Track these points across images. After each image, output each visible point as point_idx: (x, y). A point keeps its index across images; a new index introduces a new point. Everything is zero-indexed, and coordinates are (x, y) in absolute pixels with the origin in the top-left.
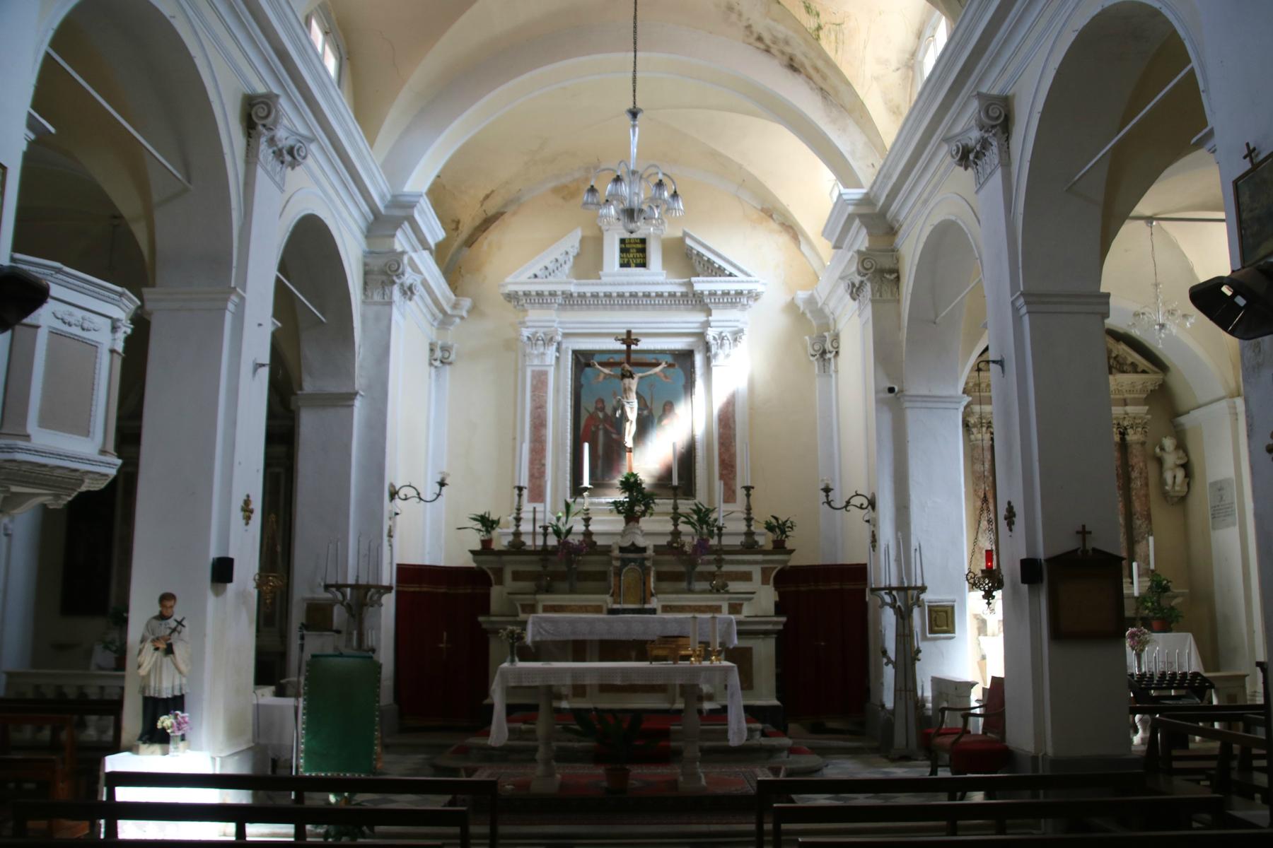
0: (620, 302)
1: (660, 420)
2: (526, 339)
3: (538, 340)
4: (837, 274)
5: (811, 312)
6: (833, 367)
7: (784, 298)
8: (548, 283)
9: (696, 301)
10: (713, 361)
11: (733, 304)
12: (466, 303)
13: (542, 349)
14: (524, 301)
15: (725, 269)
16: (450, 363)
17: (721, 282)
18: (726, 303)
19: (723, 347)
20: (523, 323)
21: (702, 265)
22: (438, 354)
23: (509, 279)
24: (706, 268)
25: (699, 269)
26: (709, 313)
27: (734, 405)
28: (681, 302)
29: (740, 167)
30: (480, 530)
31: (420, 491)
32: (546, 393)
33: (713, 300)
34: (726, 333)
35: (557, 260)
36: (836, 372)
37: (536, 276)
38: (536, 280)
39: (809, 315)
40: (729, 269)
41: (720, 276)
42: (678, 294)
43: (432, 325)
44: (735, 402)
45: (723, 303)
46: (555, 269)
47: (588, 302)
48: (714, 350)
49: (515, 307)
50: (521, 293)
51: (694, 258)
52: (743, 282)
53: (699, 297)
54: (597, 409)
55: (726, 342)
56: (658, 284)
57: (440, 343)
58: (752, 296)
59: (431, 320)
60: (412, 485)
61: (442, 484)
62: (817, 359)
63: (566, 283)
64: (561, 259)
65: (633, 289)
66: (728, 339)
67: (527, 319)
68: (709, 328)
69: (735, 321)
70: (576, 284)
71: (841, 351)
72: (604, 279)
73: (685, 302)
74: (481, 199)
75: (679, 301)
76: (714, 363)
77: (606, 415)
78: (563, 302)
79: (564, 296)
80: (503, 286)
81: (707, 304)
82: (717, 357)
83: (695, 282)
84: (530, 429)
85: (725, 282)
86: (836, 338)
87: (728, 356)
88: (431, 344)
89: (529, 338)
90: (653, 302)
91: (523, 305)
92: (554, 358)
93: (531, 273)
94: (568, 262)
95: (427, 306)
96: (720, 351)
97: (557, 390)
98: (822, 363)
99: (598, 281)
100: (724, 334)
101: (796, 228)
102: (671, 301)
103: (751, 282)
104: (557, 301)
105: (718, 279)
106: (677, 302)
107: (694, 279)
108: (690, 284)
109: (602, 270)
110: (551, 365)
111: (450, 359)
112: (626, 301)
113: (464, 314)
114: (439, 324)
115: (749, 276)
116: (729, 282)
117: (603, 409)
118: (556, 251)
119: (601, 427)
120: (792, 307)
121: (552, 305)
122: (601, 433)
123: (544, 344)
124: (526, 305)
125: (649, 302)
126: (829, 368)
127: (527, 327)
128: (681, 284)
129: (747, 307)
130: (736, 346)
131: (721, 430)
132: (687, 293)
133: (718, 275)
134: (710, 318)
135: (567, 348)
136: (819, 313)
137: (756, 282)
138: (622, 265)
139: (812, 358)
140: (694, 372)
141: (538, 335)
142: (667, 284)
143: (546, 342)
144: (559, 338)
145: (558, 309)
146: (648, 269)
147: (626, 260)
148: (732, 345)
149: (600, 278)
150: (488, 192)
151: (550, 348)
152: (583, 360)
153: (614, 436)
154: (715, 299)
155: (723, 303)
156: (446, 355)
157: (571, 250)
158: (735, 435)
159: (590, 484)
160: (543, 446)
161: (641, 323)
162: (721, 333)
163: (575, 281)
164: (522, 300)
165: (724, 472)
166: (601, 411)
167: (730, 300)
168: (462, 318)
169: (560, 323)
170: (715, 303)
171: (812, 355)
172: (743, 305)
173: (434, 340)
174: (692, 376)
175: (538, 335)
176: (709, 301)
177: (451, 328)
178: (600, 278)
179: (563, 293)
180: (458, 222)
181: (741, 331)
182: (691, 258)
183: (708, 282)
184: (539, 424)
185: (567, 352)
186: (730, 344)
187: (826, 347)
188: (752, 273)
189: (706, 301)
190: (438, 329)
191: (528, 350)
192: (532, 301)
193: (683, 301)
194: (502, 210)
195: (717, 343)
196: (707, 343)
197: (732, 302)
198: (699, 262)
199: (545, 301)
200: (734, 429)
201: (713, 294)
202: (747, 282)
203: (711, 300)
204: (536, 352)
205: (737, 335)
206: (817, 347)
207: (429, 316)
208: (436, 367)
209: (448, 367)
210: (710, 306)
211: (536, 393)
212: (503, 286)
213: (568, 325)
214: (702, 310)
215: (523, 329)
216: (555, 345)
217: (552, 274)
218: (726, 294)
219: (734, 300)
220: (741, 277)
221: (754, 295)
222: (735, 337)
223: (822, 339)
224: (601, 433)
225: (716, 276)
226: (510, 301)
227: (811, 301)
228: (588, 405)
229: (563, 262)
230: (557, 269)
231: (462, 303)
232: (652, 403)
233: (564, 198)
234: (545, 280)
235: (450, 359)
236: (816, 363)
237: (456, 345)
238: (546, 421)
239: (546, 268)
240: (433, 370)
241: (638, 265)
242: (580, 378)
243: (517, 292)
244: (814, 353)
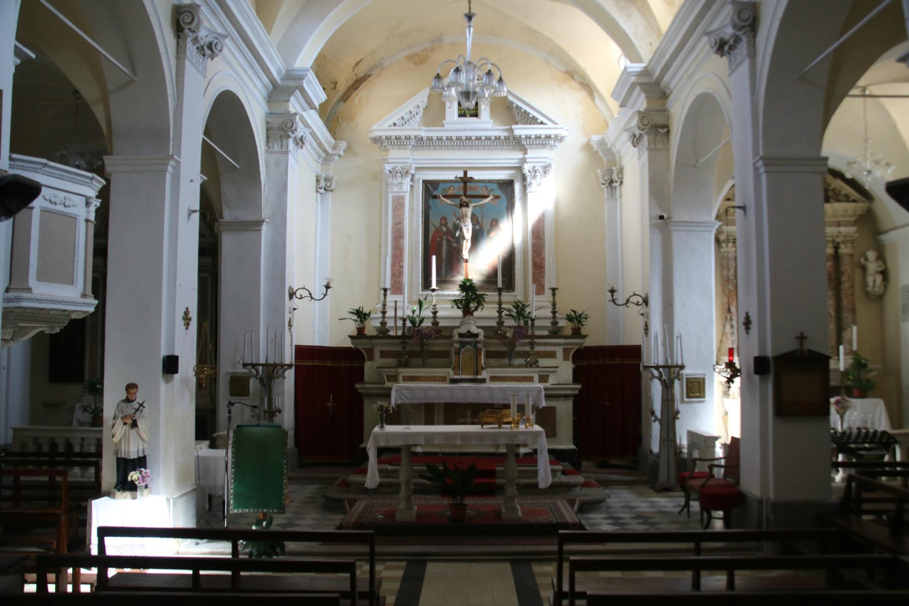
0: (458, 144)
1: (489, 232)
2: (388, 172)
3: (397, 173)
4: (622, 124)
5: (602, 151)
6: (618, 193)
7: (583, 140)
8: (404, 130)
9: (515, 143)
10: (528, 188)
11: (543, 145)
12: (343, 145)
13: (400, 180)
14: (386, 143)
15: (537, 119)
16: (331, 191)
17: (534, 128)
18: (538, 144)
19: (536, 178)
20: (385, 160)
21: (520, 116)
22: (323, 184)
23: (374, 127)
24: (523, 118)
25: (518, 118)
26: (525, 152)
27: (544, 222)
28: (504, 144)
29: (550, 39)
30: (356, 321)
31: (311, 292)
32: (404, 213)
33: (528, 143)
34: (539, 167)
35: (411, 112)
36: (621, 196)
37: (395, 124)
38: (395, 128)
39: (600, 154)
40: (541, 118)
41: (534, 124)
42: (502, 138)
43: (318, 162)
44: (544, 219)
45: (536, 144)
46: (410, 118)
47: (434, 144)
48: (529, 180)
49: (379, 148)
50: (384, 138)
51: (514, 109)
52: (551, 128)
53: (517, 140)
54: (441, 224)
55: (538, 174)
56: (487, 130)
57: (324, 175)
58: (558, 139)
59: (317, 159)
60: (305, 288)
61: (328, 287)
62: (606, 187)
63: (417, 130)
64: (414, 112)
65: (469, 134)
66: (539, 172)
67: (388, 157)
68: (525, 164)
69: (545, 158)
70: (425, 131)
71: (625, 182)
72: (446, 127)
73: (508, 144)
74: (353, 66)
75: (503, 143)
76: (529, 190)
77: (448, 229)
78: (416, 144)
79: (417, 139)
80: (370, 132)
81: (524, 146)
82: (531, 185)
83: (515, 129)
84: (392, 240)
85: (538, 128)
86: (621, 171)
87: (539, 184)
88: (317, 176)
89: (390, 171)
90: (483, 144)
91: (385, 146)
92: (409, 186)
93: (391, 122)
94: (419, 114)
95: (313, 148)
96: (533, 181)
97: (411, 210)
98: (610, 191)
99: (442, 128)
100: (536, 168)
101: (591, 87)
102: (497, 143)
103: (557, 128)
104: (411, 143)
105: (532, 126)
106: (501, 144)
107: (514, 127)
108: (511, 130)
109: (445, 119)
110: (407, 192)
111: (331, 188)
112: (463, 143)
113: (342, 153)
114: (322, 161)
115: (556, 124)
116: (541, 128)
117: (446, 225)
118: (410, 106)
119: (444, 238)
120: (588, 147)
121: (407, 146)
122: (444, 243)
123: (402, 176)
124: (388, 146)
125: (480, 144)
126: (615, 193)
127: (389, 163)
128: (504, 130)
129: (554, 147)
130: (546, 177)
131: (534, 241)
132: (509, 136)
133: (532, 123)
134: (526, 156)
135: (419, 178)
136: (609, 152)
137: (560, 128)
138: (460, 116)
139: (602, 186)
140: (514, 197)
141: (397, 169)
142: (493, 130)
143: (403, 175)
144: (413, 171)
145: (412, 149)
146: (480, 118)
147: (463, 111)
148: (542, 176)
149: (443, 126)
150: (358, 60)
151: (406, 179)
152: (430, 188)
153: (454, 245)
154: (530, 142)
155: (536, 144)
156: (329, 184)
157: (422, 104)
158: (544, 244)
159: (437, 286)
160: (401, 253)
161: (475, 159)
162: (534, 167)
163: (424, 128)
164: (385, 142)
165: (536, 272)
167: (541, 142)
168: (340, 156)
169: (414, 159)
170: (530, 144)
171: (603, 184)
172: (551, 146)
173: (320, 173)
174: (512, 201)
175: (397, 169)
176: (525, 143)
177: (332, 164)
178: (443, 126)
179: (416, 137)
180: (336, 83)
181: (550, 165)
182: (512, 110)
183: (524, 128)
184: (398, 236)
185: (419, 182)
186: (541, 175)
187: (613, 178)
188: (558, 122)
189: (523, 143)
190: (322, 164)
191: (390, 181)
192: (393, 143)
193: (506, 143)
194: (369, 73)
195: (531, 175)
196: (524, 175)
197: (542, 144)
198: (518, 113)
199: (402, 143)
200: (544, 240)
201: (528, 137)
202: (554, 128)
203: (527, 142)
204: (395, 182)
205: (546, 169)
206: (606, 178)
207: (315, 156)
208: (321, 194)
209: (330, 193)
210: (526, 146)
211: (396, 213)
212: (370, 132)
213: (419, 162)
214: (520, 150)
215: (386, 165)
216: (410, 176)
217: (407, 123)
218: (538, 137)
219: (544, 142)
220: (550, 125)
221: (559, 138)
222: (545, 170)
223: (610, 171)
224: (444, 243)
225: (530, 124)
226: (376, 143)
227: (602, 143)
228: (435, 221)
229: (415, 114)
230: (411, 118)
231: (340, 145)
232: (482, 220)
233: (415, 63)
234: (401, 127)
235: (331, 188)
236: (605, 190)
237: (336, 177)
238: (403, 234)
239: (403, 118)
240: (319, 195)
241: (472, 116)
243: (381, 137)
244: (604, 182)
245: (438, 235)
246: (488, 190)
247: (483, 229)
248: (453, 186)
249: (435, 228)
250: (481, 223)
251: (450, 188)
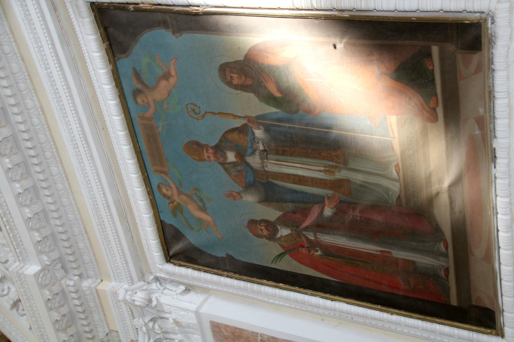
54: (272, 236)
77: (283, 221)
166: (276, 231)
174: (145, 11)
232: (235, 117)
242: (216, 258)
245: (304, 251)
246: (139, 86)
247: (258, 117)
248: (159, 187)
249: (287, 257)
250: (244, 122)
251: (165, 196)
